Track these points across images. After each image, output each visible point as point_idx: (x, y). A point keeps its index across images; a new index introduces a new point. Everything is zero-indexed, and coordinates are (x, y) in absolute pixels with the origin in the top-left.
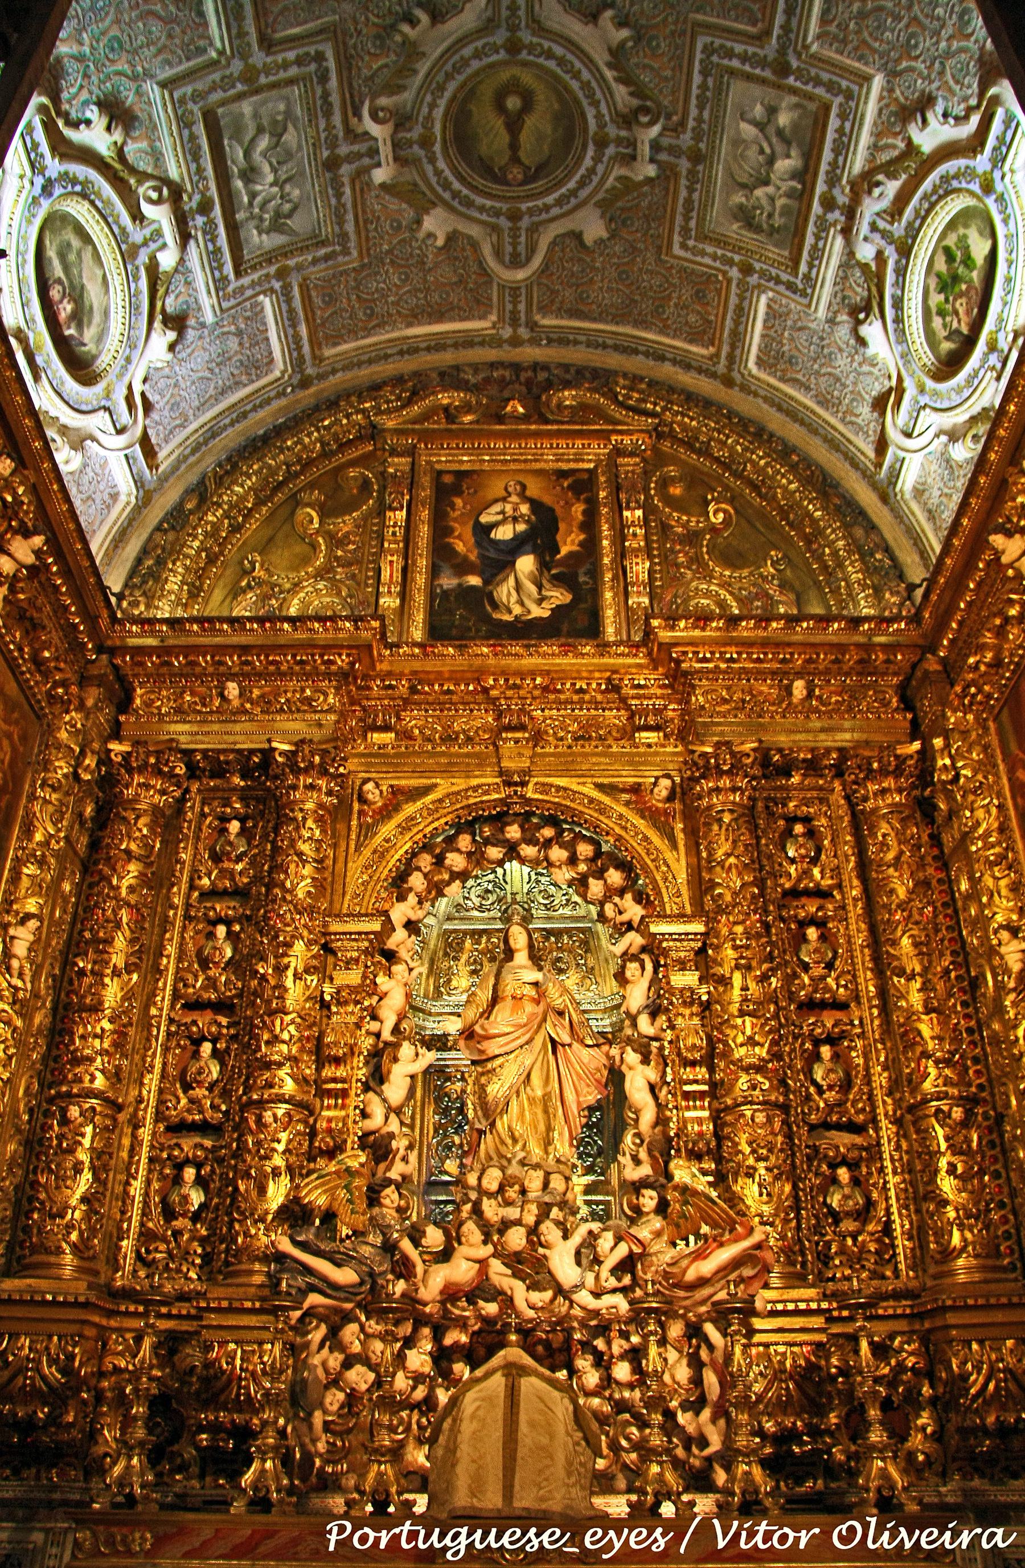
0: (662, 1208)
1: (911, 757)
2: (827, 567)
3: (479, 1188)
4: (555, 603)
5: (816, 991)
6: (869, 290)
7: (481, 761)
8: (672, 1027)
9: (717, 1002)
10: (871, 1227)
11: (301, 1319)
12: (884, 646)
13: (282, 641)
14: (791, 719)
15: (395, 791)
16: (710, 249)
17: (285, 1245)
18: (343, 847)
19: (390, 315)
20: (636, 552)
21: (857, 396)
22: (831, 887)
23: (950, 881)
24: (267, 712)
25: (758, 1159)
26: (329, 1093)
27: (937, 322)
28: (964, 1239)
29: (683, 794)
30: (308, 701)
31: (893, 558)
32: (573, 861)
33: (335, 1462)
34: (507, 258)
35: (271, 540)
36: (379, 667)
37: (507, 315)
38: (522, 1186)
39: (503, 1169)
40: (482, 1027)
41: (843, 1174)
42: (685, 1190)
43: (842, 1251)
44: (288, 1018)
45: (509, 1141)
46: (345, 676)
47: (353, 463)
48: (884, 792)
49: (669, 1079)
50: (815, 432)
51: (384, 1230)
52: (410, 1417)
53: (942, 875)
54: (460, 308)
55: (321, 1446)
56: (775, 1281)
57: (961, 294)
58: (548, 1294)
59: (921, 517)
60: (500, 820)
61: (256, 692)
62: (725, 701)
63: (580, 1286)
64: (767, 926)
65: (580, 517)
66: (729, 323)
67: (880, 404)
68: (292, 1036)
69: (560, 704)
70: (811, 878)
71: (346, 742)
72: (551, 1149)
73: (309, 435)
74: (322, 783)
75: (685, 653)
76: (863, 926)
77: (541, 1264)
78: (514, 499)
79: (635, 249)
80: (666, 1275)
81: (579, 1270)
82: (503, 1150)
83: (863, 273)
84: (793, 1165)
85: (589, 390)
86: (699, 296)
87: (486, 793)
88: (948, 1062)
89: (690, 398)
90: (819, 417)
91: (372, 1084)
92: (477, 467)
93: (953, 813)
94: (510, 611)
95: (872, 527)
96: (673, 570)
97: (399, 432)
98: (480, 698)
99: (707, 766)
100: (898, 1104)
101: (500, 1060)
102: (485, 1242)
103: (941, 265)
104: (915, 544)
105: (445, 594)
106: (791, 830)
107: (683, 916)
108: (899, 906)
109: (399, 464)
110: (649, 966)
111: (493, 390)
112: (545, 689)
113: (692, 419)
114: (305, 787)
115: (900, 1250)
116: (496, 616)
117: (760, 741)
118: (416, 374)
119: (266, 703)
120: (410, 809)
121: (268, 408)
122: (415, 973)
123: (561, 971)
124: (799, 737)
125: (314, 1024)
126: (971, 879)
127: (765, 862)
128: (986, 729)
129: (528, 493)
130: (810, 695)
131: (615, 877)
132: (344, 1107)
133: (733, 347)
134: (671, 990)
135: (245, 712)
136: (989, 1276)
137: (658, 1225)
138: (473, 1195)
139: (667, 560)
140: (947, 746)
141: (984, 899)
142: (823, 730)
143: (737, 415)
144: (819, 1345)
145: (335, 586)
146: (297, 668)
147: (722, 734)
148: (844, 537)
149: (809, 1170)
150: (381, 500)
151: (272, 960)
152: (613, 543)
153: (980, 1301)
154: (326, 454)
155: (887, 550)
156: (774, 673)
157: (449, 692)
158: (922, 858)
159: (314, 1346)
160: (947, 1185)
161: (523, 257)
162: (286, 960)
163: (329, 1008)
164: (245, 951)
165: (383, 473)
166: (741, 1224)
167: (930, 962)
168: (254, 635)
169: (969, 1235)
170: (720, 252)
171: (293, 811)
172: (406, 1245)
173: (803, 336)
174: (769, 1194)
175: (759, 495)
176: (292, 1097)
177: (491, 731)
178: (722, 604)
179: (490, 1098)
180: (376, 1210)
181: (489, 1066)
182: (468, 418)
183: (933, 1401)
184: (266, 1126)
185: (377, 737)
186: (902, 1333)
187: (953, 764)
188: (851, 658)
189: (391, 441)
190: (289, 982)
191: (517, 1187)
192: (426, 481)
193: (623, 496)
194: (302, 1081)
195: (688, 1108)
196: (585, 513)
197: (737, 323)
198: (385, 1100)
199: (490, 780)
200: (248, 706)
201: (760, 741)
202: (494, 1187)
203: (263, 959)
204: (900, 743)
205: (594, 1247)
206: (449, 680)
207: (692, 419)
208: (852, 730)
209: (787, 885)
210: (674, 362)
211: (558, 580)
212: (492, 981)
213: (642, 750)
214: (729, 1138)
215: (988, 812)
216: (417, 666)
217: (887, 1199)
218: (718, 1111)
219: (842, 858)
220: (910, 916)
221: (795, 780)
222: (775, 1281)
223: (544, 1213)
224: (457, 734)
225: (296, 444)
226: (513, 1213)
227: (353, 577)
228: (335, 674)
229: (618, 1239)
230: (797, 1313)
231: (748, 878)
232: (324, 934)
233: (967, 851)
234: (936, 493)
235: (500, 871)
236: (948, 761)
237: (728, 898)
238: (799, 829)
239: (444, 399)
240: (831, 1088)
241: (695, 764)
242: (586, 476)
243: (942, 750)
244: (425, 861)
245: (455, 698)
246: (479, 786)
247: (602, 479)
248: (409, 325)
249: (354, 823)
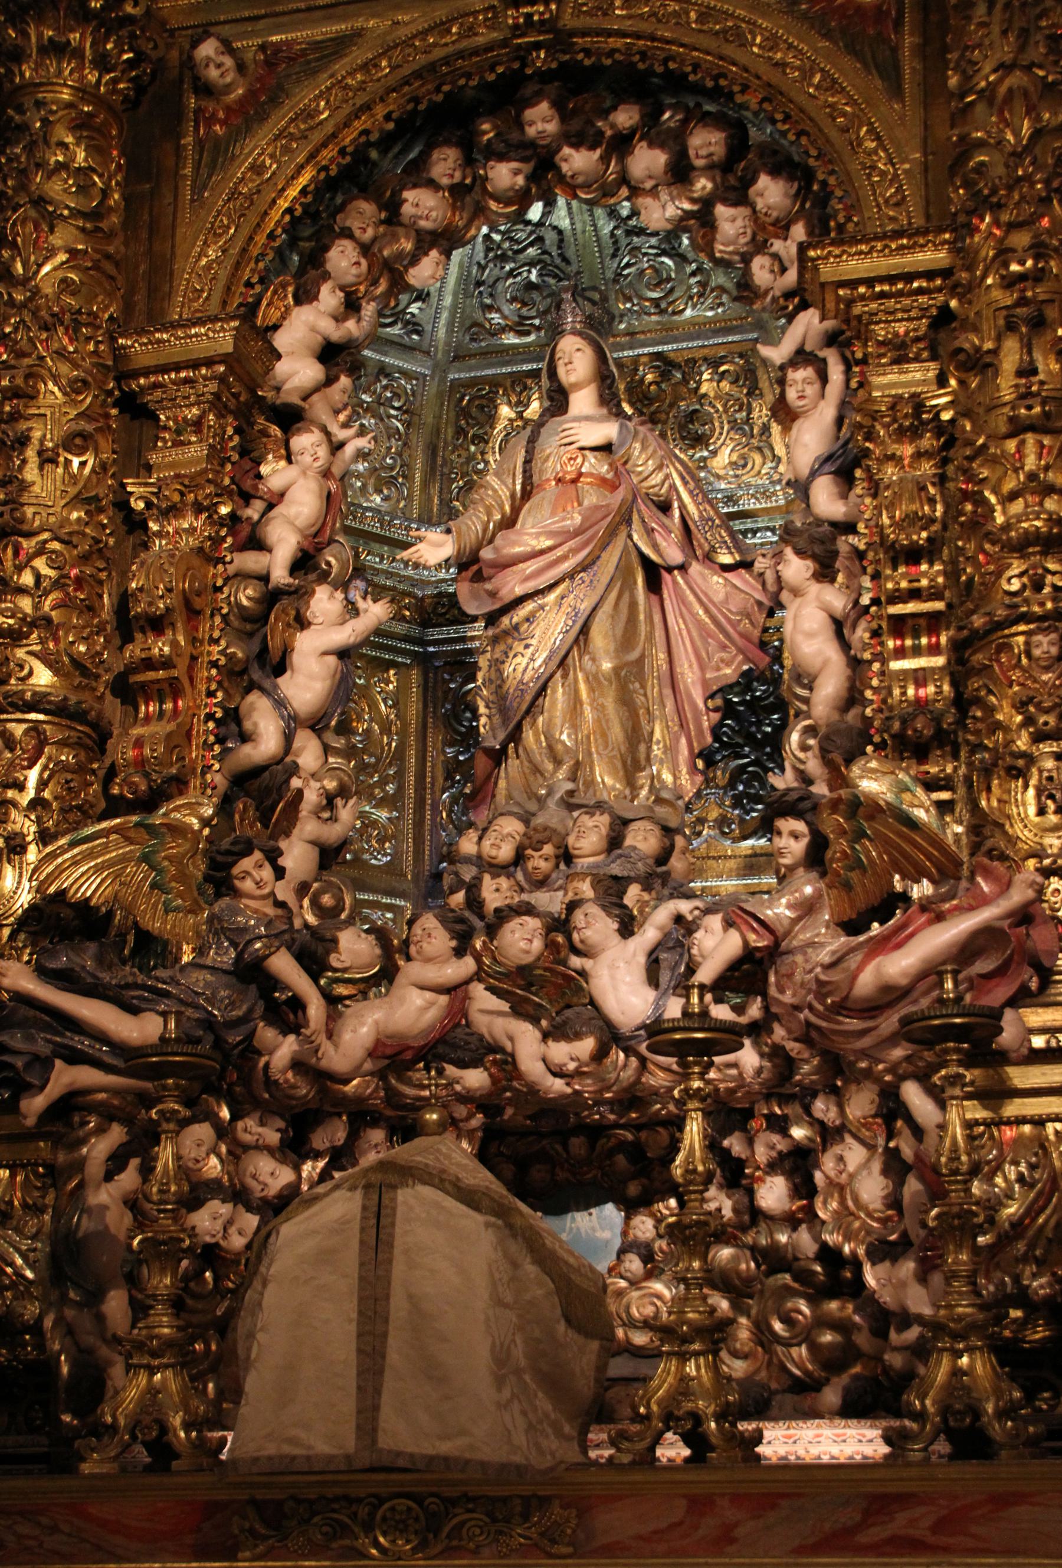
15: (273, 56)
18: (169, 199)
39: (526, 819)
58: (587, 1046)
80: (822, 988)
81: (651, 995)
101: (529, 607)
102: (459, 952)
120: (305, 96)
122: (349, 450)
123: (699, 441)
137: (808, 890)
179: (511, 685)
181: (505, 621)
191: (548, 849)
195: (900, 653)
198: (280, 704)
202: (505, 852)
214: (978, 702)
235: (550, 237)
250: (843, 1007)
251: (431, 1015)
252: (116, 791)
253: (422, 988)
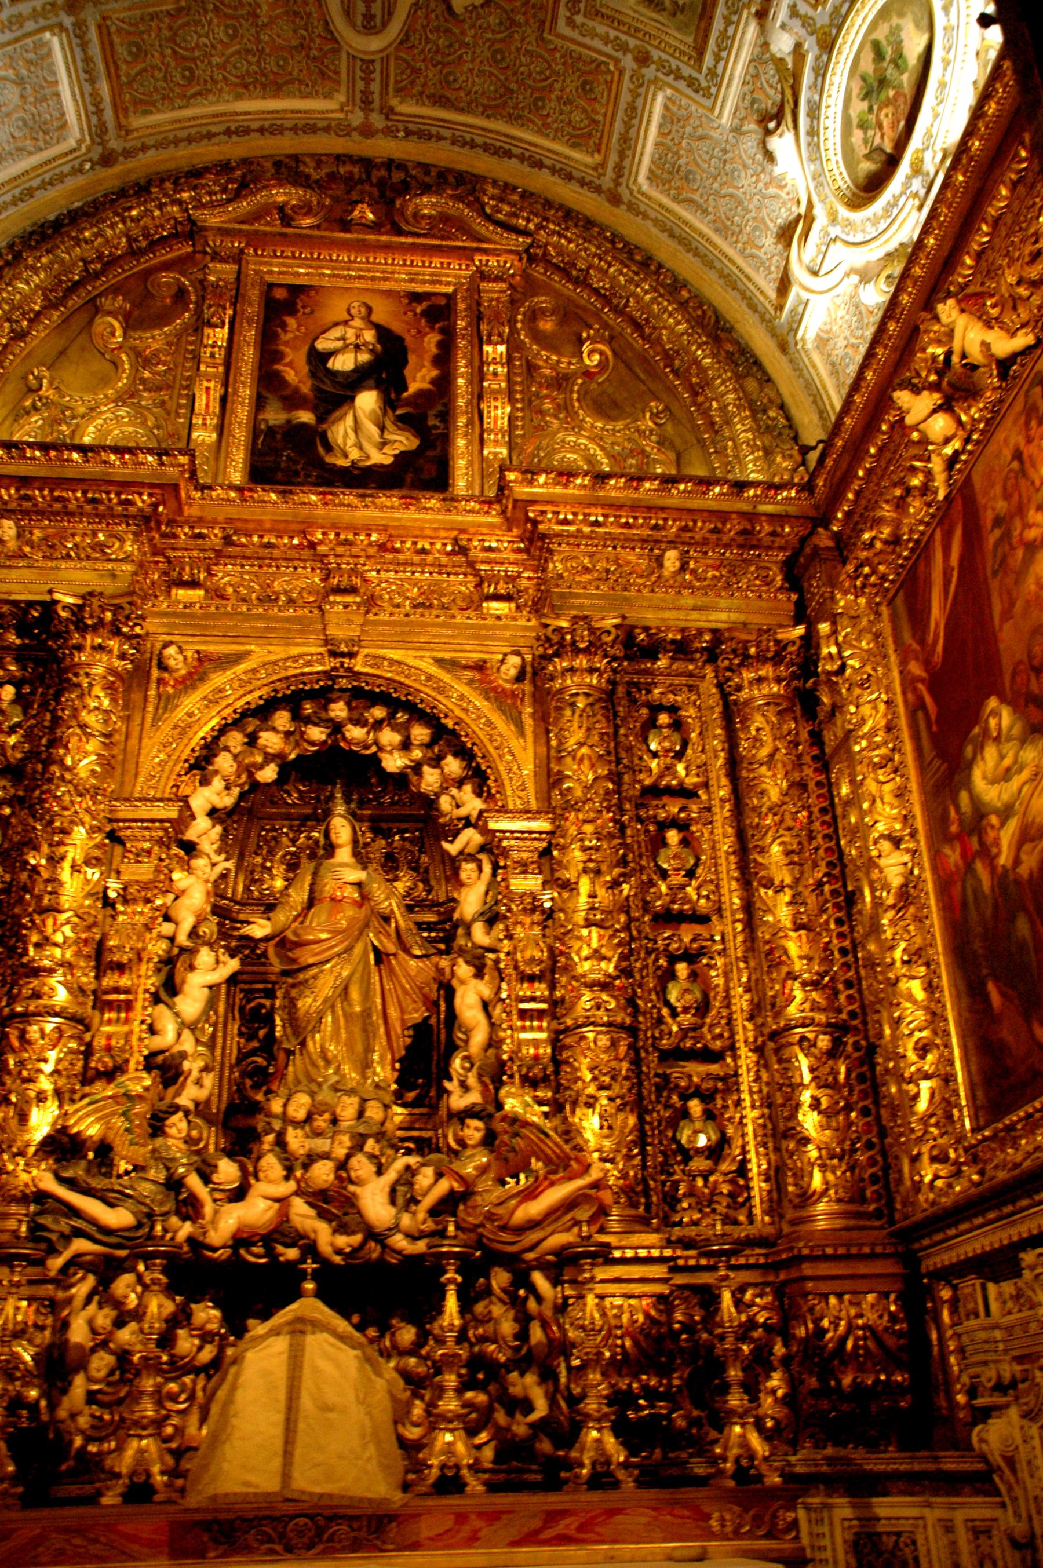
0: (489, 1140)
1: (793, 642)
2: (713, 424)
3: (284, 1117)
4: (397, 450)
5: (673, 902)
6: (783, 93)
7: (304, 627)
8: (510, 937)
9: (561, 910)
10: (724, 1167)
11: (64, 1270)
12: (771, 517)
13: (70, 474)
14: (660, 594)
15: (202, 658)
16: (601, 29)
17: (49, 1184)
19: (215, 82)
20: (495, 394)
21: (760, 224)
22: (696, 786)
23: (830, 784)
24: (50, 558)
25: (601, 1088)
26: (110, 1005)
28: (826, 1182)
29: (535, 673)
30: (101, 547)
31: (788, 418)
32: (406, 745)
33: (100, 1440)
34: (359, 21)
35: (62, 353)
36: (187, 511)
37: (358, 96)
38: (334, 1114)
39: (312, 1094)
40: (295, 933)
41: (695, 1106)
42: (514, 1120)
43: (691, 1193)
44: (62, 917)
45: (321, 1063)
46: (147, 520)
47: (167, 266)
48: (760, 680)
49: (504, 995)
50: (711, 265)
51: (168, 1166)
52: (194, 1382)
53: (822, 778)
54: (301, 82)
55: (83, 1421)
56: (615, 1226)
57: (888, 103)
59: (823, 370)
60: (323, 696)
61: (37, 534)
62: (587, 570)
63: (396, 1228)
64: (623, 828)
65: (434, 350)
66: (618, 126)
67: (785, 234)
68: (66, 938)
69: (400, 565)
70: (675, 774)
71: (145, 598)
72: (369, 1072)
73: (112, 226)
74: (113, 644)
75: (543, 513)
76: (730, 830)
77: (350, 1203)
78: (357, 323)
79: (513, 23)
80: (490, 1217)
81: (393, 1211)
82: (313, 1071)
83: (778, 71)
84: (640, 1097)
85: (451, 197)
86: (586, 88)
87: (309, 664)
88: (815, 985)
89: (569, 215)
91: (163, 995)
92: (315, 282)
93: (836, 708)
94: (346, 456)
95: (767, 380)
96: (537, 419)
97: (223, 232)
98: (306, 553)
99: (562, 643)
100: (759, 1028)
101: (315, 970)
102: (287, 1178)
103: (867, 65)
104: (815, 402)
105: (271, 431)
106: (656, 720)
107: (528, 812)
108: (770, 809)
109: (220, 272)
110: (487, 868)
111: (338, 190)
112: (382, 547)
113: (570, 241)
114: (93, 648)
115: (756, 1193)
116: (329, 459)
117: (624, 617)
118: (246, 162)
119: (51, 548)
120: (218, 679)
121: (60, 187)
124: (668, 614)
125: (95, 924)
126: (852, 782)
127: (623, 754)
128: (878, 614)
129: (374, 318)
130: (683, 568)
131: (453, 765)
132: (127, 1021)
133: (622, 155)
134: (510, 896)
135: (24, 556)
136: (852, 1223)
138: (277, 1125)
139: (531, 405)
140: (834, 632)
141: (866, 805)
142: (694, 608)
143: (622, 239)
144: (660, 1298)
145: (139, 412)
146: (88, 508)
147: (580, 607)
148: (735, 390)
149: (658, 1102)
150: (198, 313)
151: (45, 849)
152: (470, 382)
153: (841, 1251)
154: (134, 253)
155: (782, 407)
156: (644, 541)
157: (269, 545)
158: (799, 757)
159: (78, 1302)
160: (809, 1121)
161: (378, 21)
162: (62, 849)
163: (114, 908)
164: (16, 839)
165: (202, 282)
166: (577, 1159)
167: (802, 873)
168: (36, 465)
169: (831, 1177)
170: (613, 33)
171: (76, 675)
172: (194, 1181)
173: (704, 146)
174: (610, 1127)
175: (642, 336)
176: (64, 1009)
177: (318, 593)
178: (590, 460)
180: (159, 1141)
181: (301, 976)
182: (308, 221)
183: (786, 1362)
184: (30, 1043)
185: (181, 594)
186: (755, 1285)
187: (839, 653)
188: (732, 528)
189: (214, 242)
190: (65, 873)
191: (327, 1116)
192: (254, 294)
193: (484, 327)
194: (78, 991)
195: (524, 1029)
196: (440, 345)
197: (628, 126)
198: (177, 1015)
199: (313, 650)
200: (27, 549)
201: (624, 617)
202: (301, 1115)
203: (36, 848)
204: (781, 626)
205: (411, 1184)
206: (270, 531)
207: (570, 241)
208: (729, 610)
209: (647, 782)
210: (553, 170)
211: (405, 422)
212: (308, 879)
213: (490, 621)
214: (567, 1063)
215: (875, 708)
216: (233, 512)
217: (743, 1135)
218: (558, 1032)
219: (711, 754)
220: (782, 821)
221: (662, 663)
222: (615, 1226)
223: (358, 1146)
224: (277, 594)
225: (96, 235)
226: (322, 1145)
227: (163, 403)
228: (134, 517)
229: (439, 1175)
230: (636, 1260)
231: (602, 771)
232: (110, 820)
233: (849, 751)
234: (842, 343)
236: (834, 650)
237: (578, 793)
238: (663, 719)
239: (279, 195)
240: (686, 1010)
241: (548, 639)
242: (443, 302)
243: (828, 637)
244: (235, 740)
245: (276, 553)
246: (300, 656)
247: (461, 306)
248: (239, 97)
249: (152, 693)
250: (504, 1228)
251: (270, 1214)
252: (93, 1064)
253: (266, 1198)
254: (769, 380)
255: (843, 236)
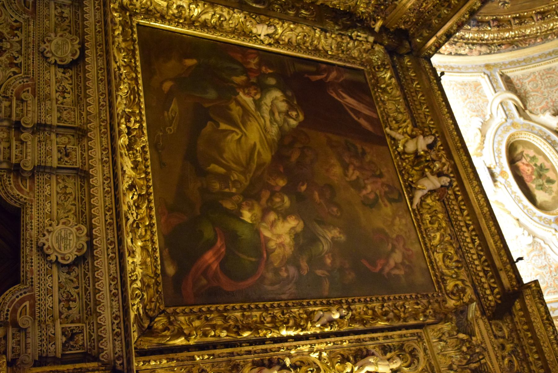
27: (532, 153)
31: (460, 55)
50: (540, 56)
57: (532, 174)
90: (545, 64)
104: (458, 68)
155: (466, 55)
254: (480, 54)
255: (504, 125)
